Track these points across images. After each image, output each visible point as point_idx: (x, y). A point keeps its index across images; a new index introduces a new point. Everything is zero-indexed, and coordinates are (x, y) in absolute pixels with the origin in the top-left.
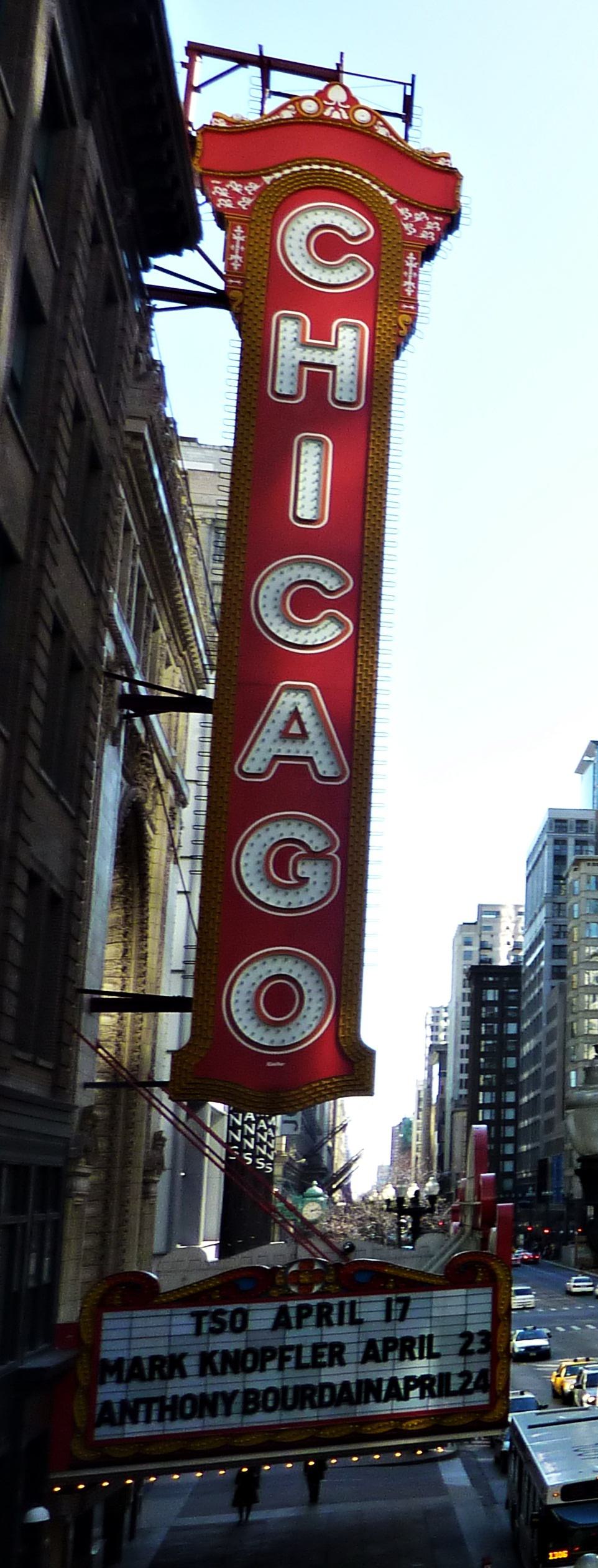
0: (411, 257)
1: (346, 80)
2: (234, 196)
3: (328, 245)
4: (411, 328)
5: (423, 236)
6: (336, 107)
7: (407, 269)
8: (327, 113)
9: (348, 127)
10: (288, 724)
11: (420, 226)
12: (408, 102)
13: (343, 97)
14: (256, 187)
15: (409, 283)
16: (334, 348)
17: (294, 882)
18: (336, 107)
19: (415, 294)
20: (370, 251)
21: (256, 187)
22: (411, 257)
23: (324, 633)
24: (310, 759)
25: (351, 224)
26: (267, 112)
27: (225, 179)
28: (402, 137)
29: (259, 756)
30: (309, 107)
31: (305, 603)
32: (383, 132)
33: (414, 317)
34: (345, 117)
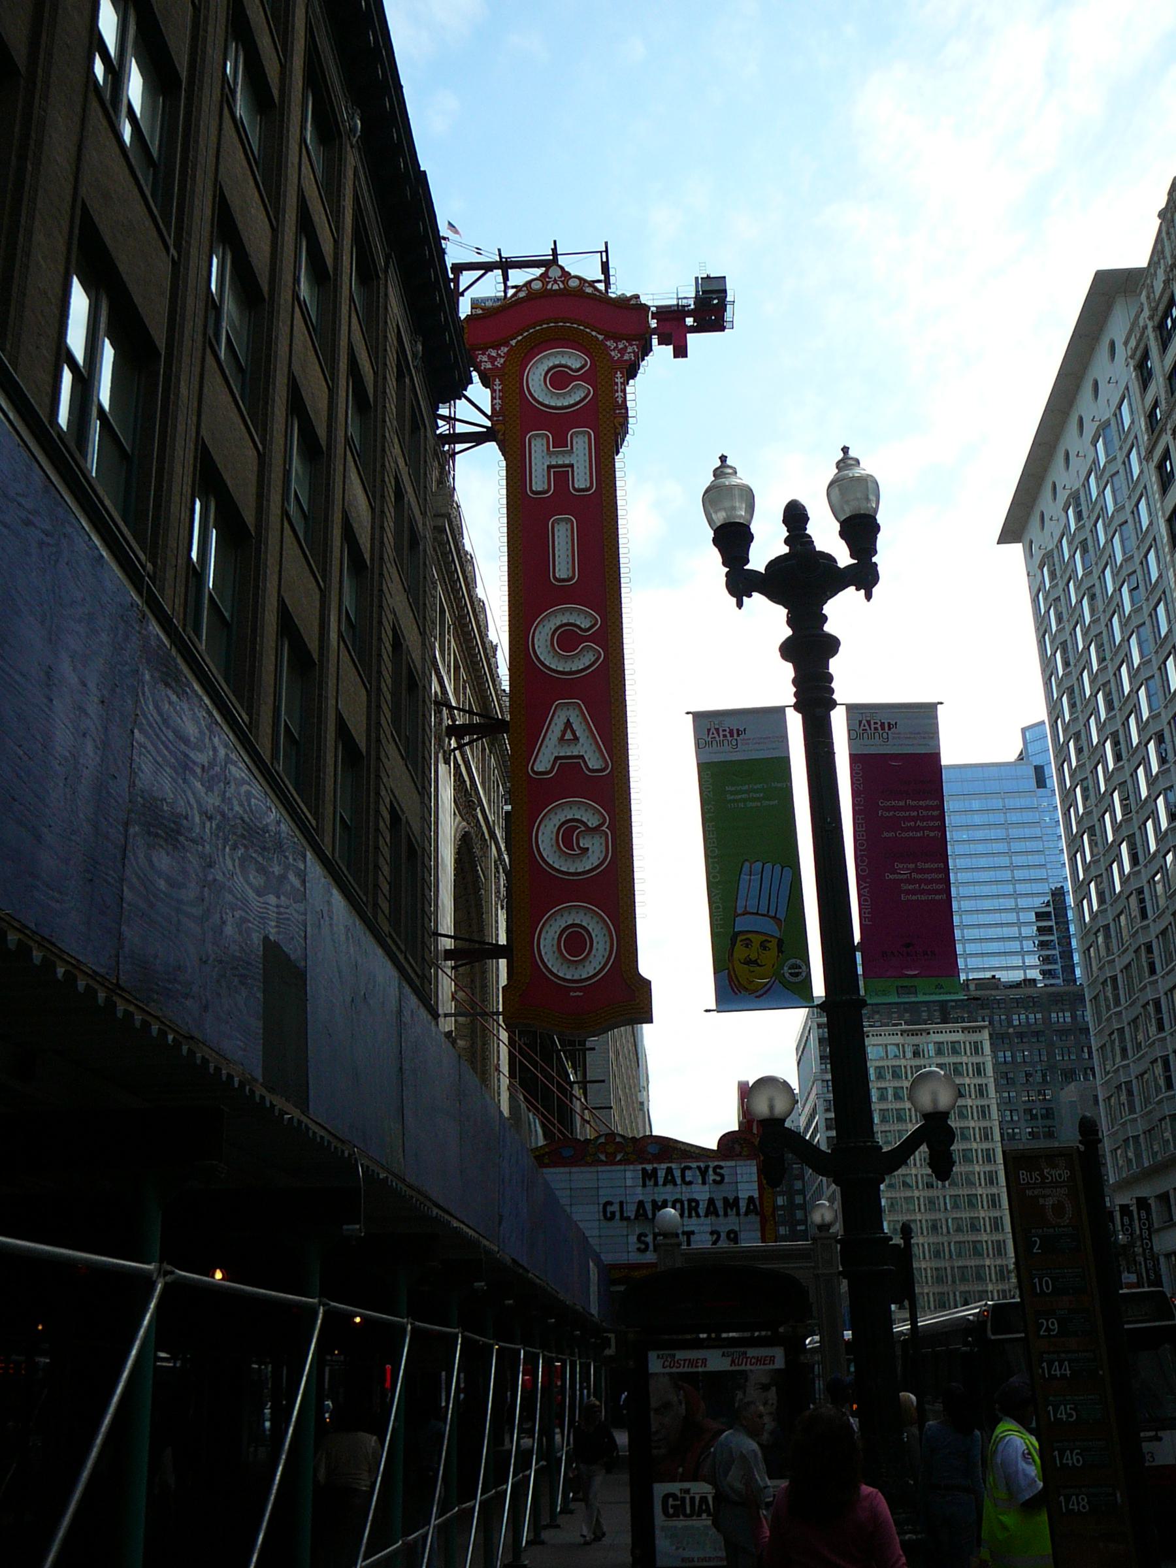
0: (619, 375)
1: (561, 260)
2: (492, 359)
3: (559, 379)
5: (626, 358)
6: (555, 281)
7: (616, 384)
8: (549, 287)
9: (566, 293)
10: (564, 733)
11: (622, 351)
12: (605, 267)
14: (506, 349)
17: (578, 852)
18: (555, 281)
20: (588, 377)
21: (506, 349)
22: (619, 375)
23: (583, 661)
25: (574, 360)
27: (484, 350)
29: (543, 763)
30: (537, 285)
34: (562, 286)
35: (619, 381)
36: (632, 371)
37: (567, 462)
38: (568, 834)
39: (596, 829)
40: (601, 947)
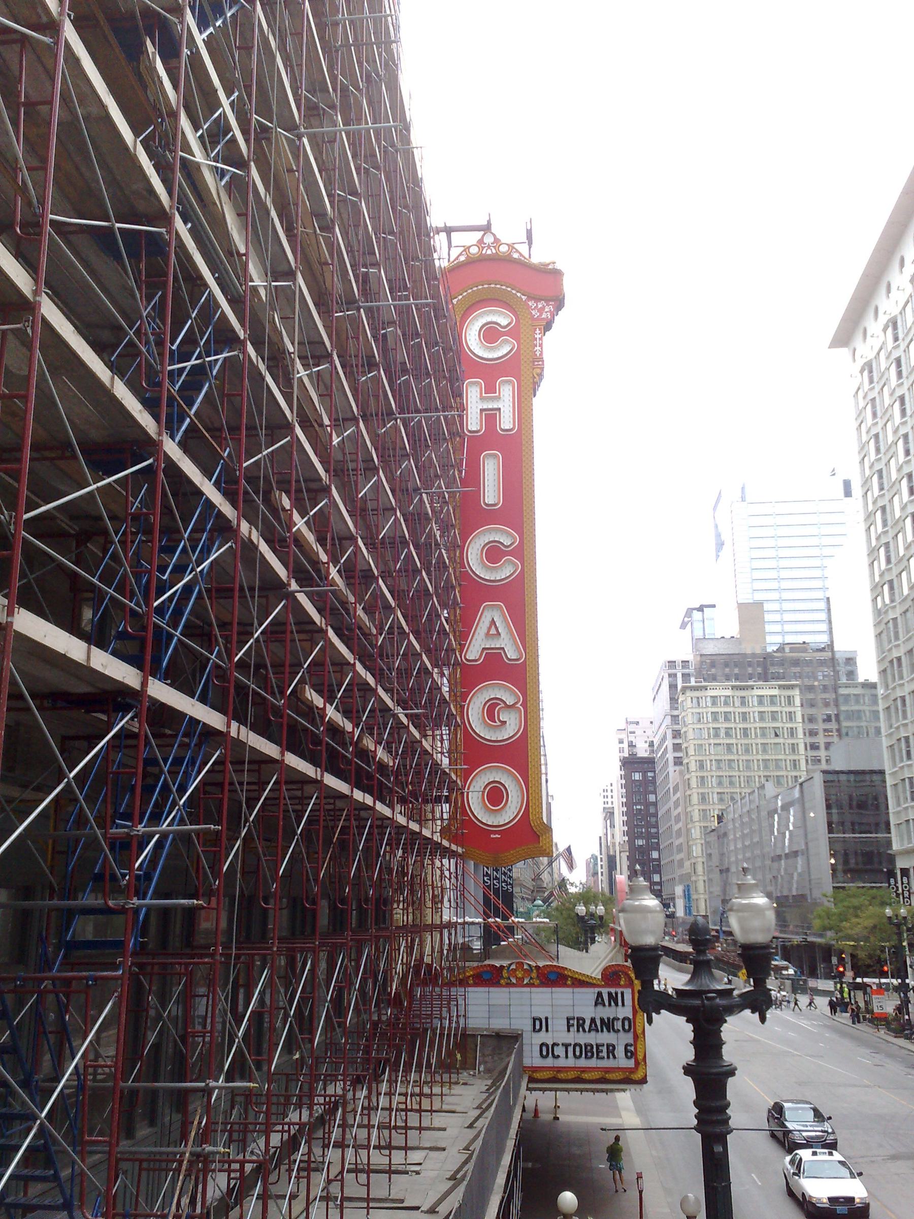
0: (538, 331)
3: (490, 334)
4: (541, 376)
6: (489, 247)
9: (496, 259)
10: (489, 628)
11: (541, 310)
13: (492, 240)
15: (538, 348)
16: (499, 398)
18: (489, 247)
19: (541, 354)
20: (514, 332)
22: (538, 331)
24: (503, 649)
26: (452, 260)
28: (527, 257)
30: (474, 250)
31: (494, 554)
32: (516, 256)
33: (542, 369)
34: (494, 251)
35: (538, 336)
36: (548, 326)
37: (495, 406)
38: (491, 709)
39: (512, 706)
40: (514, 803)
